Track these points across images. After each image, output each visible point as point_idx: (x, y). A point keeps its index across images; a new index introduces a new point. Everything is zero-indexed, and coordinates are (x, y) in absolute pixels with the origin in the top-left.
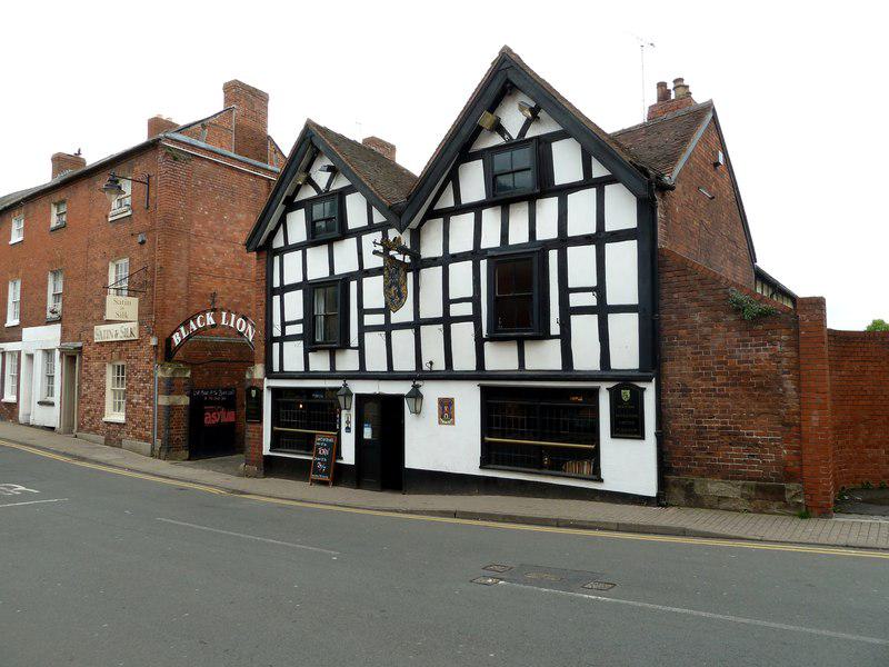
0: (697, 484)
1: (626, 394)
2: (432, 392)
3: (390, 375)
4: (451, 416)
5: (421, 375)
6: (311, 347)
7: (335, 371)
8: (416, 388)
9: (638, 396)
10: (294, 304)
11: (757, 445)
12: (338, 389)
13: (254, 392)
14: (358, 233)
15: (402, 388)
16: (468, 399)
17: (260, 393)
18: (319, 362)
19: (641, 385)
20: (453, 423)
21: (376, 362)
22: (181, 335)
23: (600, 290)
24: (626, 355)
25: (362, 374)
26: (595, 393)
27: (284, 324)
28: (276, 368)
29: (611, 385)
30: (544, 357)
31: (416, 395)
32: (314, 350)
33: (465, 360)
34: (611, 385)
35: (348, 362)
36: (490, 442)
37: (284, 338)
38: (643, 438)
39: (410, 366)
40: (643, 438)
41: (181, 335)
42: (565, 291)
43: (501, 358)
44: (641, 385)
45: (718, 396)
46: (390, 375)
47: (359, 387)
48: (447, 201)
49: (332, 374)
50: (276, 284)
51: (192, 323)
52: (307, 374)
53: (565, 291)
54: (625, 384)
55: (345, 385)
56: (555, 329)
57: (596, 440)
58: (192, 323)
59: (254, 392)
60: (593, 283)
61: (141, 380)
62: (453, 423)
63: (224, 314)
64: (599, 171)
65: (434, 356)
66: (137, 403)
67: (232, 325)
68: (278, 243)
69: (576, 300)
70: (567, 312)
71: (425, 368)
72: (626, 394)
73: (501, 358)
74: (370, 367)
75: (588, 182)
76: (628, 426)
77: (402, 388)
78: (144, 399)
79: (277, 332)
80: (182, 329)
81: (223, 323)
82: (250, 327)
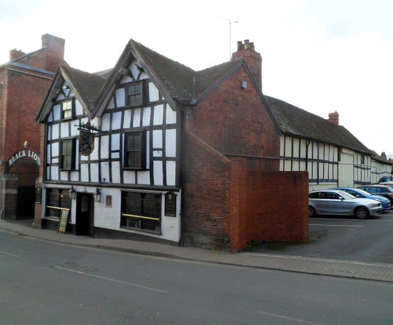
0: (195, 237)
1: (170, 197)
2: (106, 192)
3: (89, 184)
5: (101, 185)
7: (70, 181)
9: (175, 197)
10: (55, 149)
11: (216, 221)
12: (69, 189)
15: (92, 190)
16: (116, 195)
17: (41, 190)
18: (64, 177)
19: (176, 193)
22: (12, 161)
23: (163, 150)
24: (171, 181)
26: (159, 196)
27: (52, 158)
28: (48, 179)
29: (165, 192)
30: (144, 179)
31: (99, 193)
32: (63, 171)
33: (116, 180)
34: (165, 192)
35: (75, 177)
36: (125, 216)
38: (175, 216)
40: (175, 216)
41: (12, 161)
42: (152, 150)
43: (129, 178)
44: (176, 193)
45: (204, 199)
47: (81, 189)
48: (112, 106)
49: (69, 182)
50: (49, 139)
53: (152, 150)
54: (171, 191)
55: (72, 188)
56: (148, 167)
57: (159, 216)
60: (161, 147)
62: (111, 207)
65: (105, 175)
68: (50, 120)
69: (156, 154)
70: (153, 159)
71: (103, 181)
72: (170, 197)
73: (129, 178)
76: (171, 212)
79: (49, 162)
80: (13, 157)
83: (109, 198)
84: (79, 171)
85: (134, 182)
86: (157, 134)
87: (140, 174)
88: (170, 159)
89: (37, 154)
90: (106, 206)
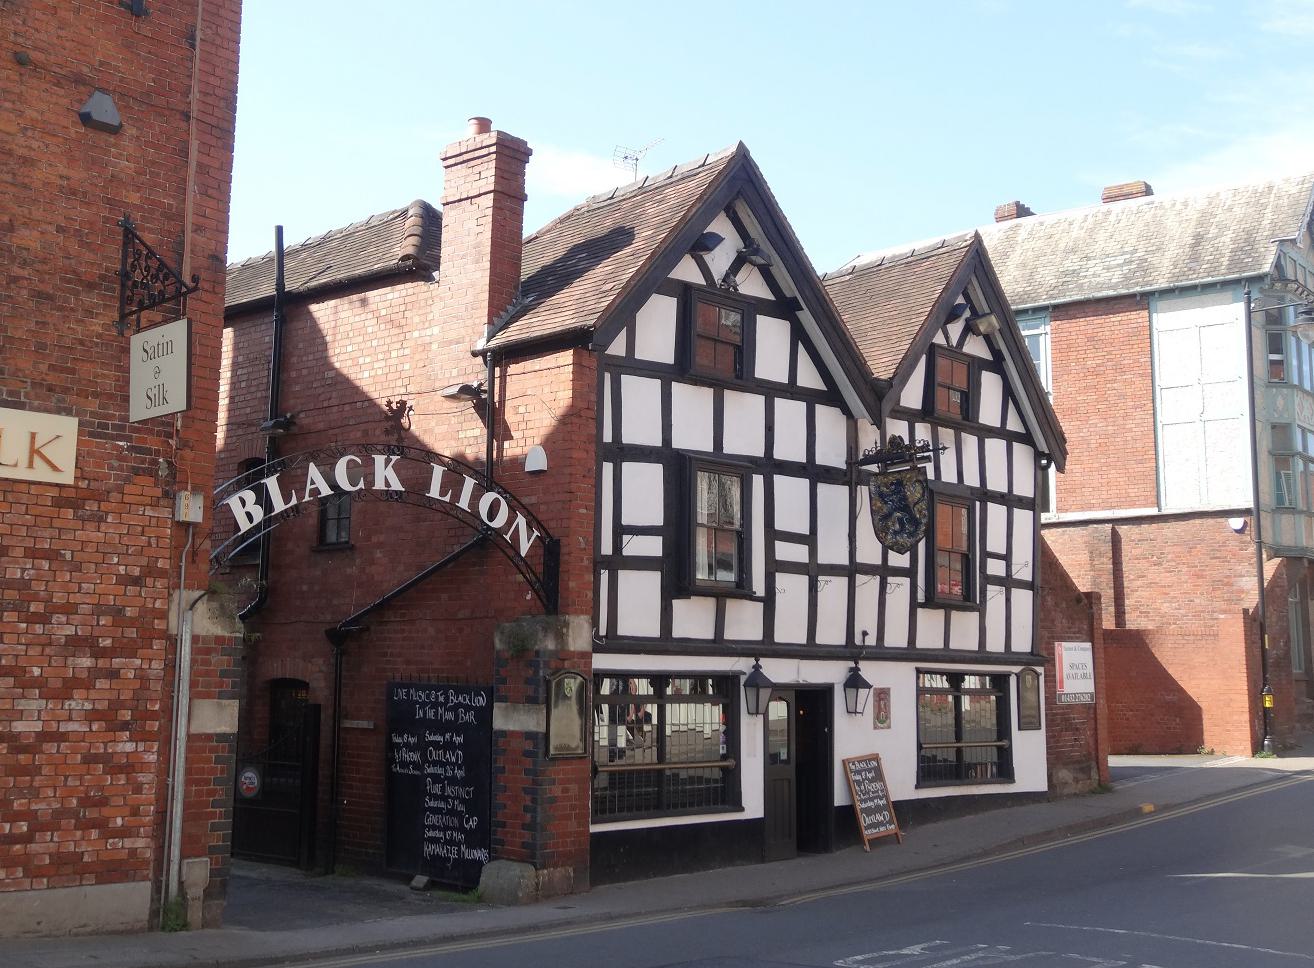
4: (887, 717)
6: (678, 582)
8: (855, 671)
14: (771, 391)
15: (830, 673)
20: (889, 727)
21: (790, 629)
22: (264, 500)
25: (767, 647)
27: (620, 530)
34: (1017, 669)
37: (619, 562)
41: (264, 500)
46: (811, 651)
49: (717, 646)
51: (313, 471)
52: (666, 643)
55: (757, 667)
58: (313, 471)
60: (1003, 552)
61: (75, 644)
64: (1014, 424)
65: (866, 620)
66: (44, 736)
67: (464, 503)
68: (618, 348)
71: (858, 641)
72: (1029, 678)
74: (781, 636)
75: (1001, 433)
77: (830, 673)
78: (91, 716)
79: (607, 548)
81: (434, 492)
82: (521, 521)
83: (882, 695)
84: (769, 601)
85: (940, 645)
86: (996, 513)
87: (733, 607)
88: (1022, 584)
89: (504, 492)
90: (875, 728)
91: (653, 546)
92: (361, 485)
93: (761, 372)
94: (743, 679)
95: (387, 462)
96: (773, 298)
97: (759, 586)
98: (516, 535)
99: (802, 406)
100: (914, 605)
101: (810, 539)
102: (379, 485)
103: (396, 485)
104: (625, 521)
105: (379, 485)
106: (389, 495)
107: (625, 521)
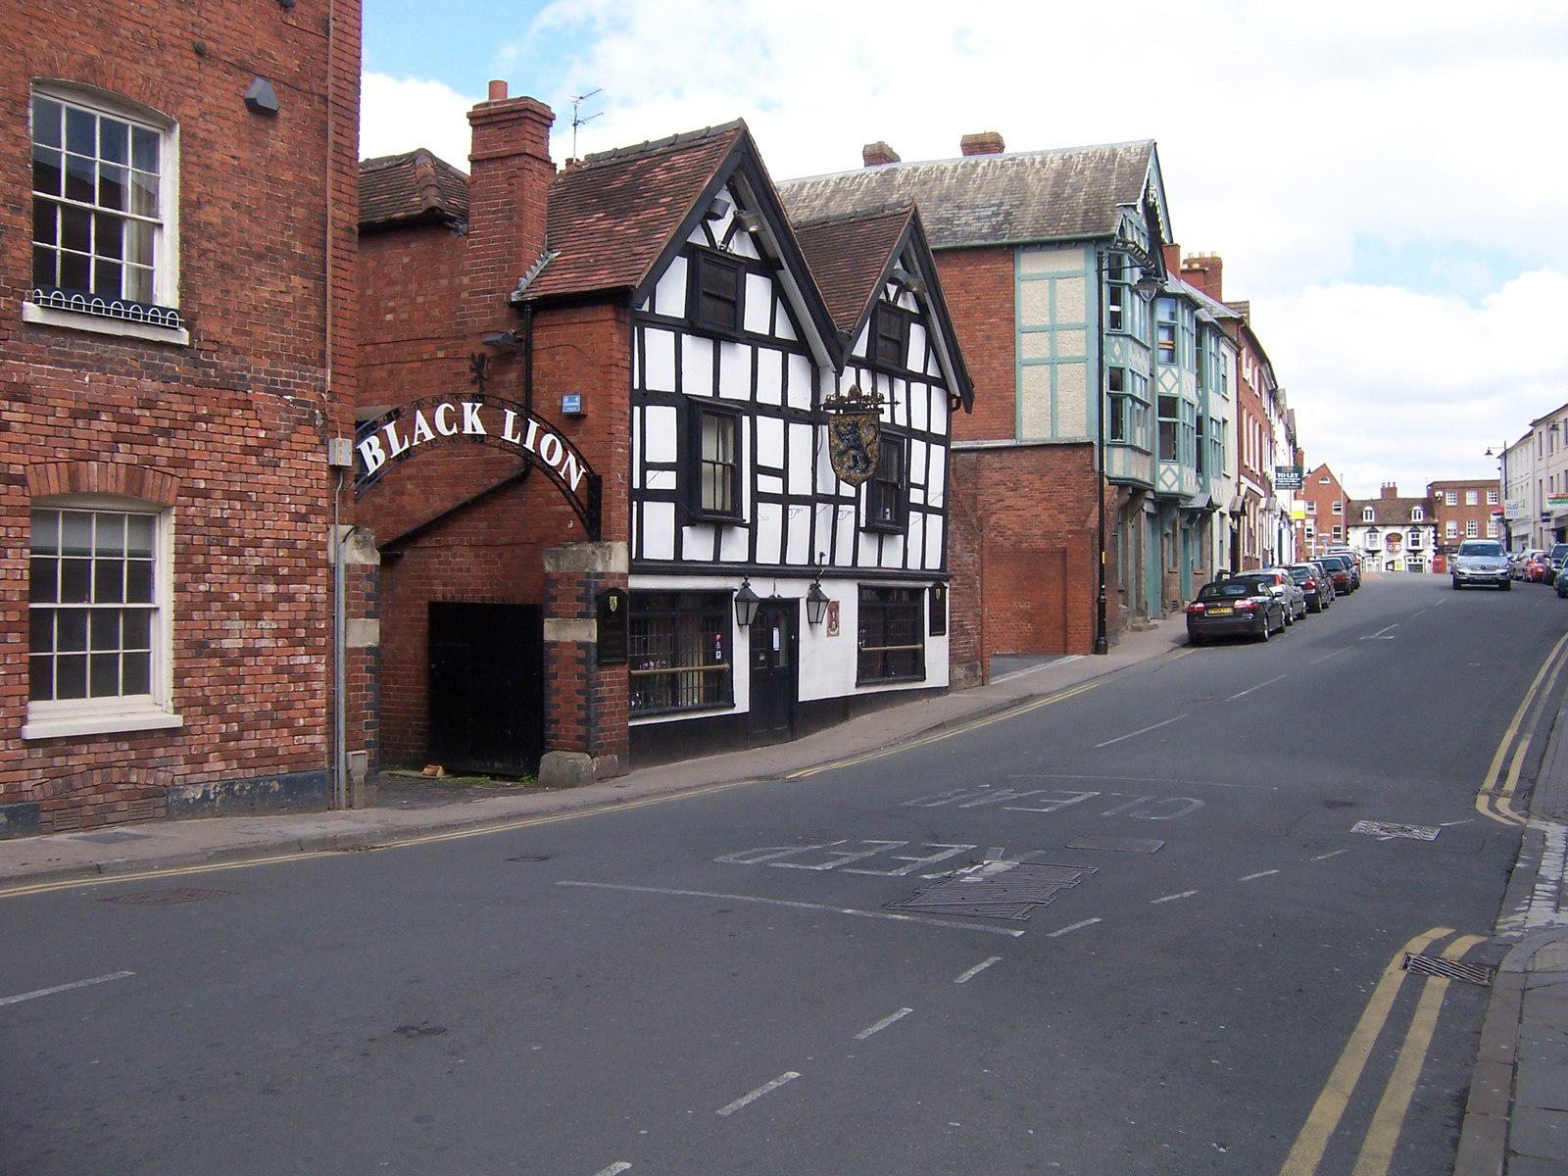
3: (782, 571)
8: (815, 588)
12: (728, 593)
13: (614, 600)
14: (756, 341)
15: (796, 589)
18: (698, 546)
21: (768, 554)
22: (385, 445)
27: (646, 466)
29: (930, 584)
32: (692, 524)
34: (930, 584)
35: (735, 549)
37: (646, 495)
39: (774, 559)
41: (385, 445)
46: (782, 571)
51: (420, 418)
52: (678, 566)
55: (746, 586)
58: (420, 418)
59: (614, 600)
60: (922, 483)
61: (265, 573)
63: (510, 415)
64: (932, 372)
65: (822, 545)
66: (246, 652)
67: (529, 445)
71: (817, 561)
72: (938, 591)
76: (937, 628)
77: (796, 589)
78: (278, 634)
80: (390, 429)
81: (508, 436)
82: (572, 459)
83: (834, 607)
86: (918, 447)
88: (935, 511)
89: (558, 434)
90: (829, 635)
91: (666, 481)
92: (455, 430)
93: (750, 325)
94: (735, 594)
95: (474, 407)
96: (759, 258)
97: (746, 516)
98: (568, 473)
99: (778, 354)
100: (857, 529)
101: (783, 473)
102: (468, 430)
103: (481, 430)
104: (648, 459)
105: (468, 430)
106: (474, 437)
107: (648, 459)
